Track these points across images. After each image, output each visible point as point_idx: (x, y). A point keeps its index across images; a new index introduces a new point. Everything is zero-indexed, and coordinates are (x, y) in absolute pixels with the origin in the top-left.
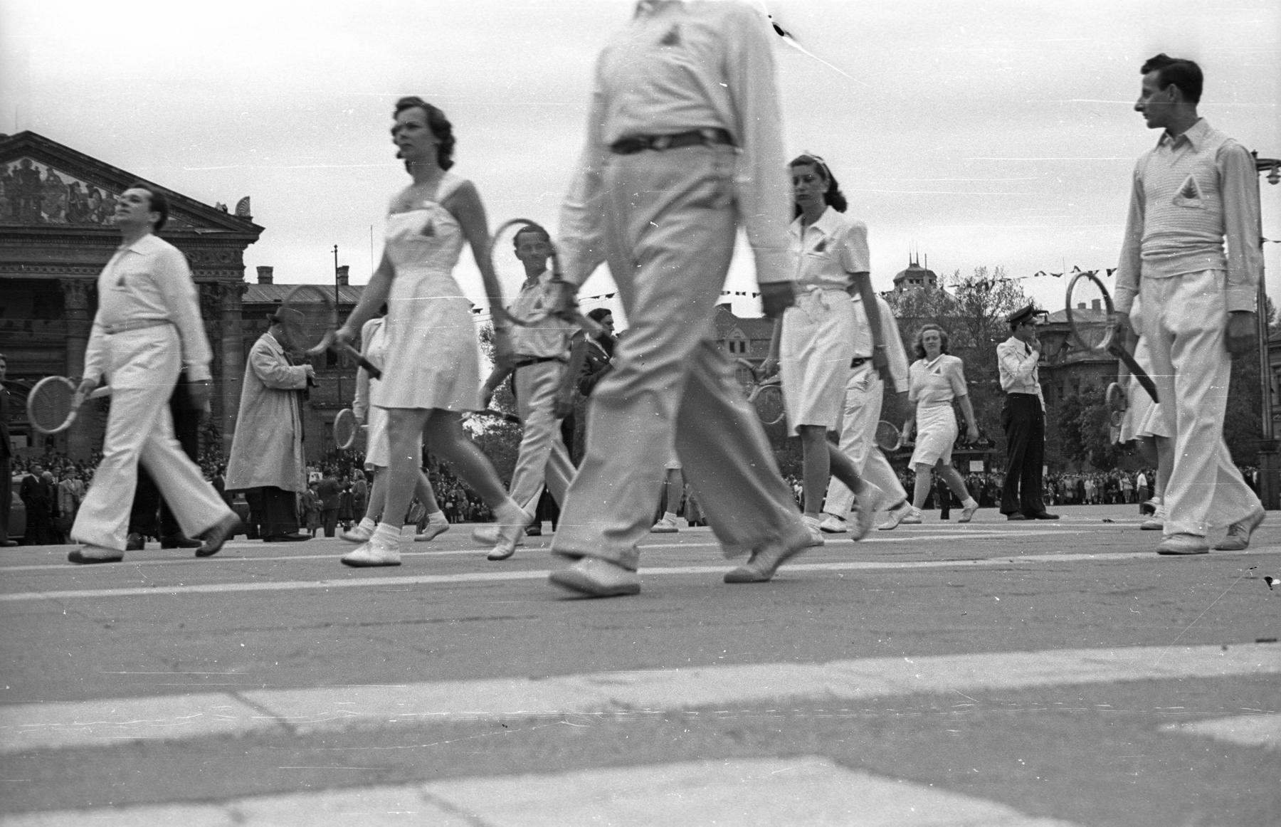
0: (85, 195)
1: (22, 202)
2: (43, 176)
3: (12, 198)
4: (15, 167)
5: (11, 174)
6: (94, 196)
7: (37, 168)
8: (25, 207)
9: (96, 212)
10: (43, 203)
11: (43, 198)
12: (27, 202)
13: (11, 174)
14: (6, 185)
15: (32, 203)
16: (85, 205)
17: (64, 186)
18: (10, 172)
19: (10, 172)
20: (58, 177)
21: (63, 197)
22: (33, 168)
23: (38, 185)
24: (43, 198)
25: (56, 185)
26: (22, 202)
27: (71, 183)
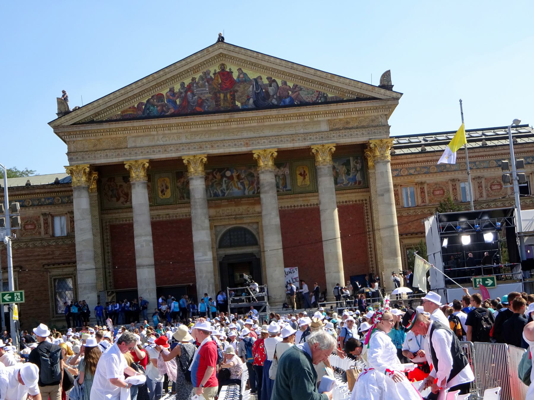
0: (266, 85)
1: (222, 96)
2: (235, 76)
3: (215, 94)
4: (215, 71)
5: (213, 76)
6: (272, 85)
7: (230, 69)
8: (224, 99)
9: (275, 97)
10: (236, 96)
11: (237, 91)
12: (225, 96)
13: (213, 76)
14: (209, 84)
15: (228, 96)
16: (267, 92)
17: (250, 81)
18: (212, 75)
19: (212, 75)
20: (245, 74)
21: (251, 89)
22: (228, 70)
23: (233, 82)
24: (237, 91)
25: (245, 80)
26: (222, 96)
27: (255, 77)
